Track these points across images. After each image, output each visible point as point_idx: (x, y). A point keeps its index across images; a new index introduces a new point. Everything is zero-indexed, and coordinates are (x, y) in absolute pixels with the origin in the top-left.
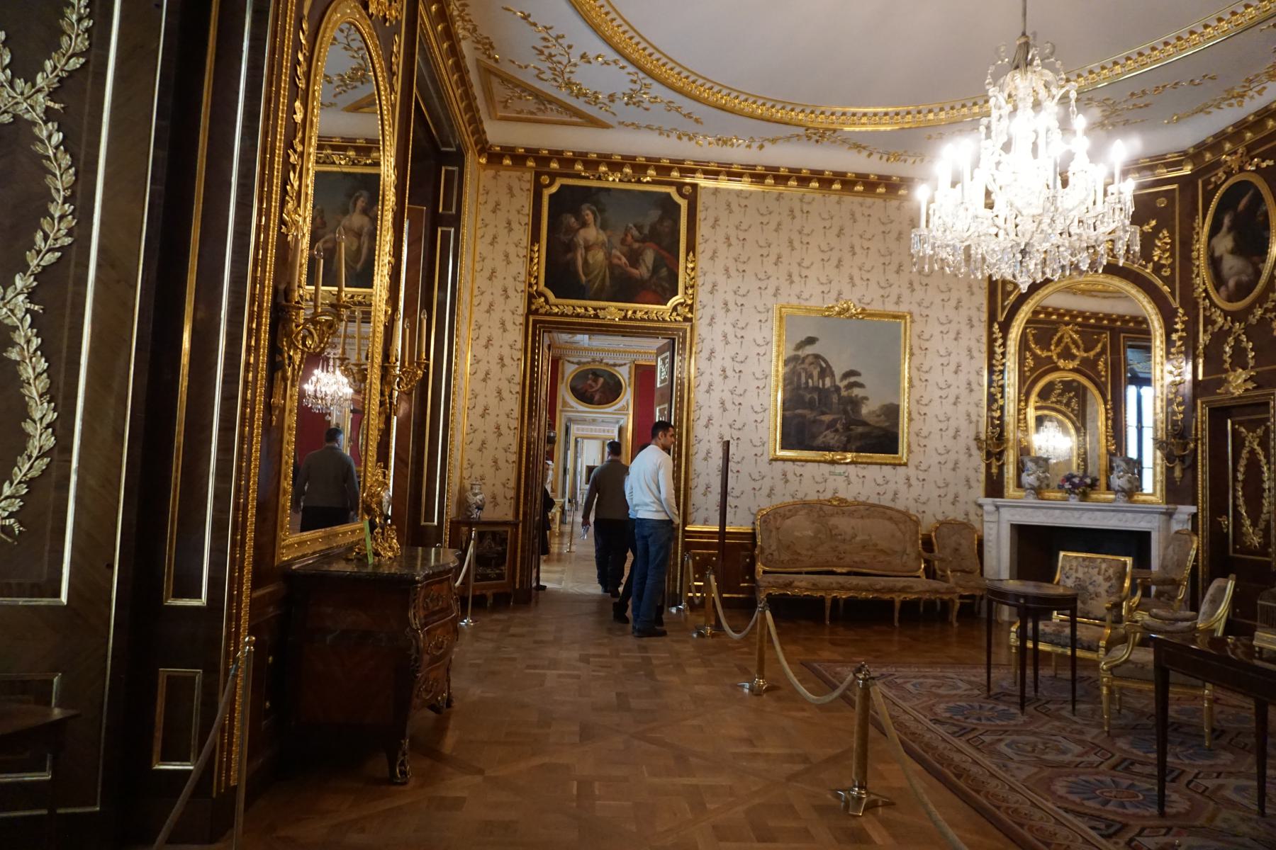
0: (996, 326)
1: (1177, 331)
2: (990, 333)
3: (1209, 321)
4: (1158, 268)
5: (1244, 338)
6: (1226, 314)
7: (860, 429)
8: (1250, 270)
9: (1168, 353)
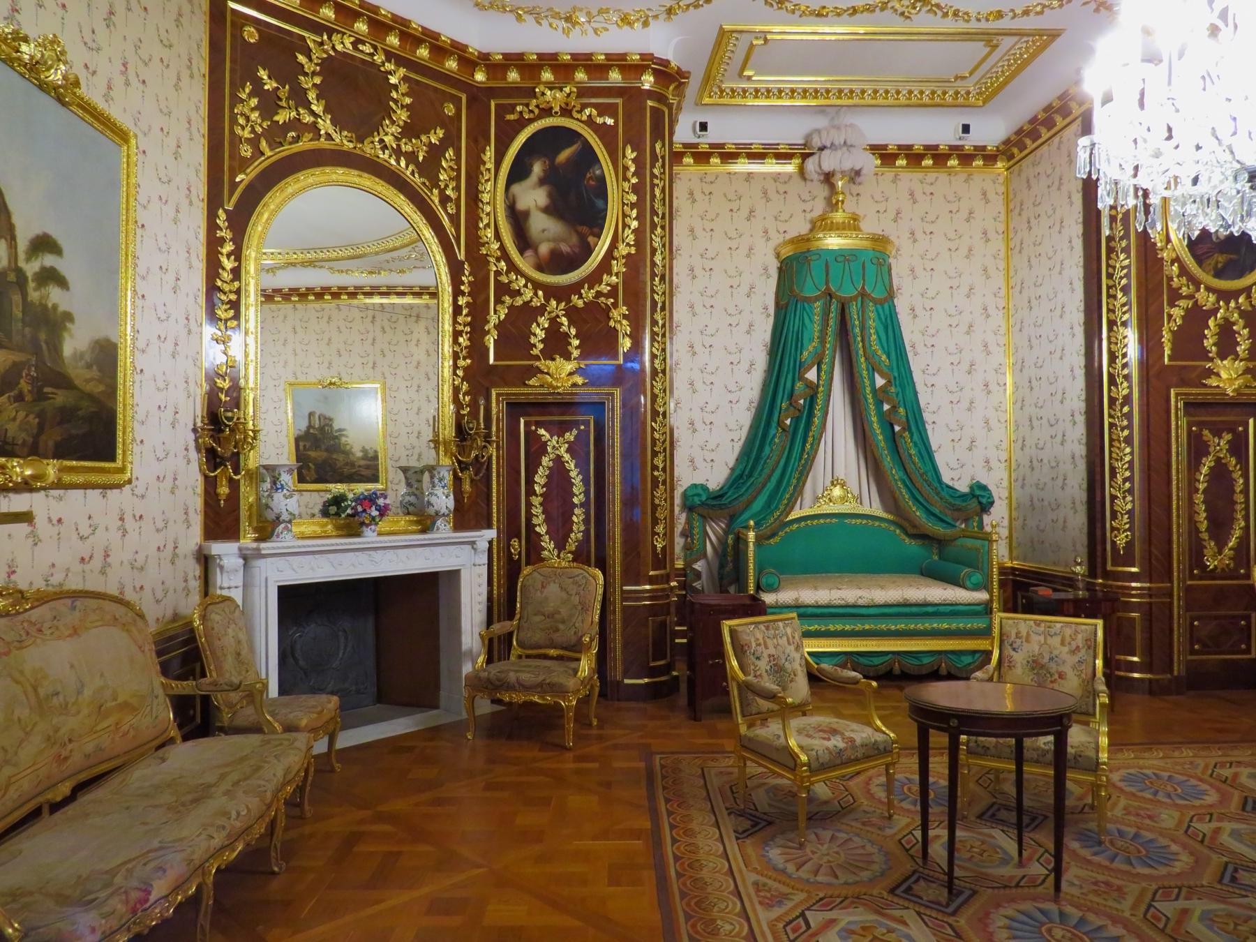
0: (222, 215)
1: (463, 293)
2: (212, 226)
3: (504, 290)
4: (444, 200)
5: (564, 320)
6: (537, 286)
7: (61, 398)
8: (574, 240)
9: (455, 322)
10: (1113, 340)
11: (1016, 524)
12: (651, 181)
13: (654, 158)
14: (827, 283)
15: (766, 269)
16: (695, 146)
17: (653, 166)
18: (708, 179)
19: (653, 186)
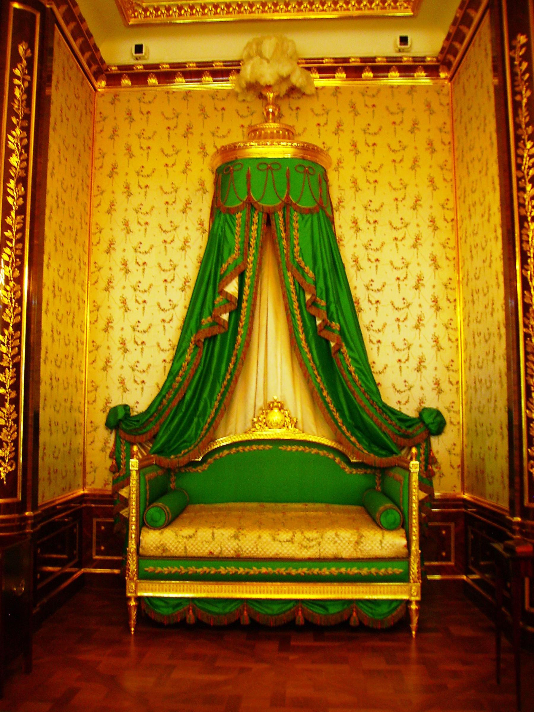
10: (524, 238)
11: (467, 451)
12: (11, 81)
13: (16, 59)
14: (249, 193)
15: (202, 184)
16: (130, 67)
17: (14, 66)
18: (147, 99)
19: (12, 86)
